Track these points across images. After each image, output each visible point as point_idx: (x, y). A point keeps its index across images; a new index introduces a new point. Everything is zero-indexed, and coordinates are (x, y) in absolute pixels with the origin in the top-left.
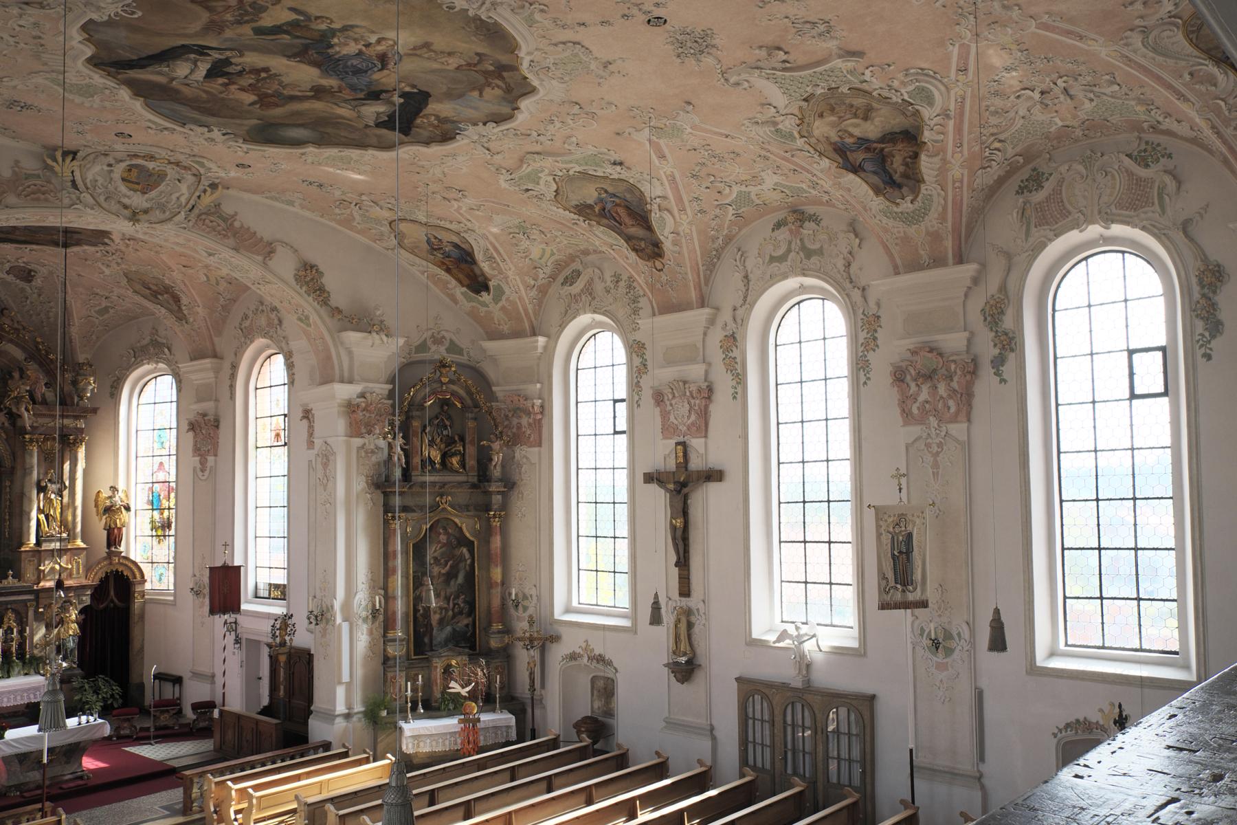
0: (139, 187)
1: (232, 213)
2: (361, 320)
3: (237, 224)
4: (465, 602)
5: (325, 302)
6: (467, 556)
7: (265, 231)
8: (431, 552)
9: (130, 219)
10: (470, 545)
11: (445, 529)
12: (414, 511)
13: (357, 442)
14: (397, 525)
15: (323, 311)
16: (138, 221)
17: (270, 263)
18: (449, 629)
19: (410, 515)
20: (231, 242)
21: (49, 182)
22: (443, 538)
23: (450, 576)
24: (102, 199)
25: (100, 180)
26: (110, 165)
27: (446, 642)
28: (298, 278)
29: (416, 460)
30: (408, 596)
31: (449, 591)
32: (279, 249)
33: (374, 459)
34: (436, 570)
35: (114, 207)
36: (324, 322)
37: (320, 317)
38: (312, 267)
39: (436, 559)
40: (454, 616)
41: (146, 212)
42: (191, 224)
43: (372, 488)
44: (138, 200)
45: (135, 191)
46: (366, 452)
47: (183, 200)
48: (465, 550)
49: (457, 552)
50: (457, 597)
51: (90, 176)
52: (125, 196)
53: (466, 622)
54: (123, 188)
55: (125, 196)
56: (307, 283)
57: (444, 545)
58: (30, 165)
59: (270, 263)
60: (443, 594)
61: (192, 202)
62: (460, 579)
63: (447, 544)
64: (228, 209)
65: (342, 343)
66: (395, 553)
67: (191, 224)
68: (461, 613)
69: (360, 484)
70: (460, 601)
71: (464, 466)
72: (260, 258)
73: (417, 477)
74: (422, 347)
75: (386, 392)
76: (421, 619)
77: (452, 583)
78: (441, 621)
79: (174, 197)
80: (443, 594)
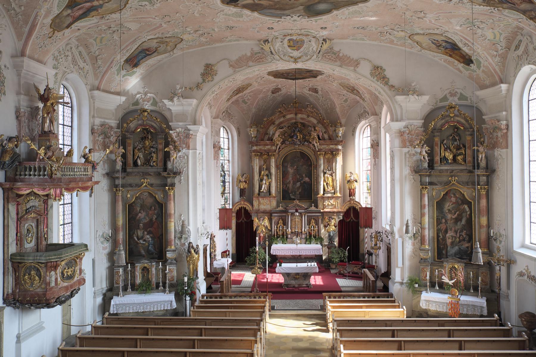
0: (294, 48)
1: (338, 50)
2: (406, 90)
3: (341, 55)
5: (386, 83)
6: (467, 209)
7: (354, 55)
8: (447, 206)
9: (294, 62)
10: (469, 204)
11: (454, 195)
12: (436, 185)
13: (406, 150)
14: (425, 192)
15: (386, 88)
16: (297, 62)
17: (357, 69)
19: (434, 187)
20: (338, 63)
21: (263, 54)
22: (453, 199)
23: (458, 220)
24: (282, 56)
25: (281, 49)
26: (282, 42)
27: (455, 254)
28: (372, 74)
29: (437, 158)
30: (434, 228)
31: (457, 228)
32: (362, 62)
33: (415, 158)
34: (449, 216)
35: (287, 58)
36: (386, 93)
37: (384, 91)
38: (378, 68)
39: (449, 210)
40: (460, 242)
41: (300, 58)
42: (320, 59)
43: (414, 173)
44: (296, 54)
45: (294, 50)
46: (410, 155)
47: (315, 49)
48: (466, 206)
49: (462, 207)
50: (462, 231)
51: (276, 49)
52: (291, 53)
53: (467, 245)
54: (289, 50)
55: (291, 53)
56: (377, 76)
57: (454, 203)
58: (256, 49)
59: (357, 69)
60: (453, 229)
61: (319, 49)
62: (464, 222)
63: (456, 203)
64: (336, 49)
65: (397, 102)
66: (425, 205)
67: (320, 59)
68: (464, 240)
69: (407, 171)
70: (463, 234)
71: (465, 161)
72: (352, 68)
73: (438, 167)
74: (445, 99)
75: (421, 124)
76: (441, 241)
77: (459, 223)
78: (452, 243)
79: (311, 49)
80: (453, 229)
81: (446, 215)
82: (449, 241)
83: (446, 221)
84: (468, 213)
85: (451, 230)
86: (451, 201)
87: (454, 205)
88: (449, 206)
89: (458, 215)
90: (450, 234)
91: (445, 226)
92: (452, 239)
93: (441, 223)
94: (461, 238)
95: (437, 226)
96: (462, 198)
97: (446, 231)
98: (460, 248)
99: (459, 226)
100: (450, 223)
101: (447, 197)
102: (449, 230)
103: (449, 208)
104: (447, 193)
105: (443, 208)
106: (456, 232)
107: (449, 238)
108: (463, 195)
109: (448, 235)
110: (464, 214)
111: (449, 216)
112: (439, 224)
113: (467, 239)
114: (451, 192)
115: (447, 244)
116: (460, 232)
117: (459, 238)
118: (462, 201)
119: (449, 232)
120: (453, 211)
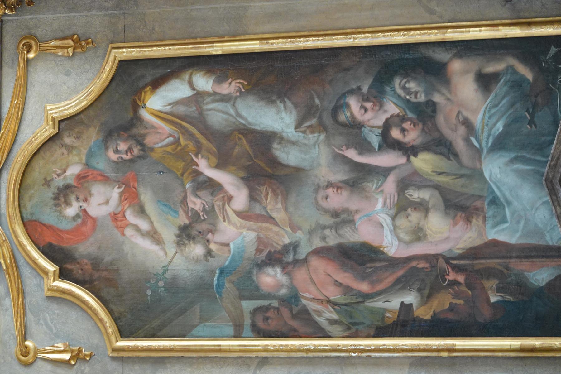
4: (376, 95)
6: (176, 91)
8: (152, 246)
10: (133, 79)
11: (63, 194)
18: (497, 171)
22: (102, 201)
23: (263, 167)
31: (326, 171)
39: (186, 234)
40: (440, 145)
48: (156, 102)
49: (161, 136)
50: (353, 131)
57: (131, 196)
60: (337, 200)
62: (274, 118)
63: (127, 177)
68: (425, 113)
70: (373, 118)
76: (443, 302)
77: (289, 157)
78: (460, 206)
80: (337, 200)
81: (223, 259)
82: (444, 235)
83: (274, 258)
84: (204, 82)
85: (343, 218)
86: (117, 218)
87: (147, 198)
88: (154, 236)
89: (220, 166)
90: (379, 225)
91: (319, 265)
92: (422, 207)
93: (292, 299)
94: (413, 136)
95: (326, 335)
96: (93, 136)
97: (360, 257)
98: (499, 145)
99: (305, 150)
100: (295, 222)
101: (85, 248)
102: (351, 236)
103: (169, 234)
104: (49, 252)
105: (173, 286)
106: (360, 177)
107: (418, 234)
108: (66, 124)
109: (392, 247)
110: (217, 116)
111: (235, 235)
112: (304, 315)
113: (415, 88)
114: (48, 217)
115: (473, 253)
116: (364, 147)
117: (411, 151)
118: (110, 134)
119: (363, 233)
120: (196, 203)
